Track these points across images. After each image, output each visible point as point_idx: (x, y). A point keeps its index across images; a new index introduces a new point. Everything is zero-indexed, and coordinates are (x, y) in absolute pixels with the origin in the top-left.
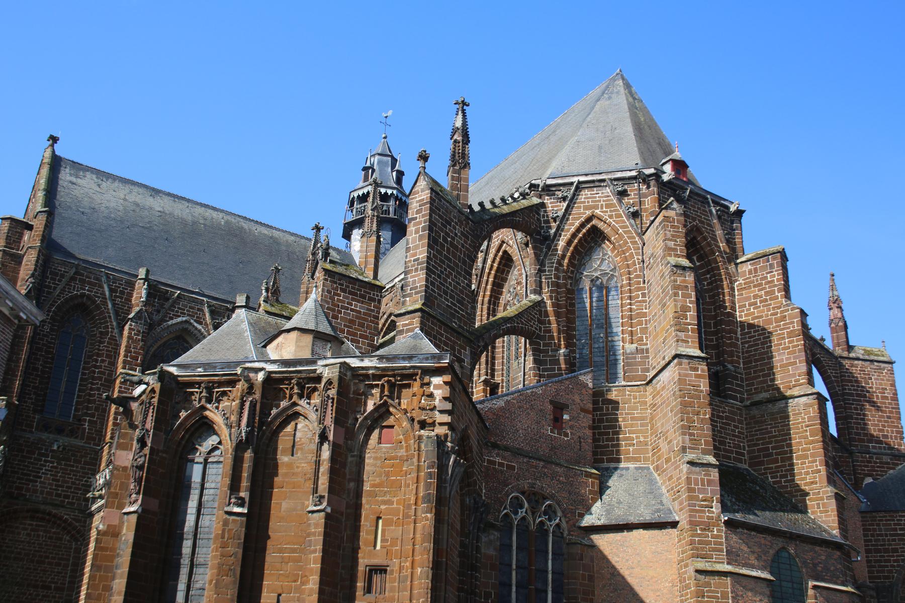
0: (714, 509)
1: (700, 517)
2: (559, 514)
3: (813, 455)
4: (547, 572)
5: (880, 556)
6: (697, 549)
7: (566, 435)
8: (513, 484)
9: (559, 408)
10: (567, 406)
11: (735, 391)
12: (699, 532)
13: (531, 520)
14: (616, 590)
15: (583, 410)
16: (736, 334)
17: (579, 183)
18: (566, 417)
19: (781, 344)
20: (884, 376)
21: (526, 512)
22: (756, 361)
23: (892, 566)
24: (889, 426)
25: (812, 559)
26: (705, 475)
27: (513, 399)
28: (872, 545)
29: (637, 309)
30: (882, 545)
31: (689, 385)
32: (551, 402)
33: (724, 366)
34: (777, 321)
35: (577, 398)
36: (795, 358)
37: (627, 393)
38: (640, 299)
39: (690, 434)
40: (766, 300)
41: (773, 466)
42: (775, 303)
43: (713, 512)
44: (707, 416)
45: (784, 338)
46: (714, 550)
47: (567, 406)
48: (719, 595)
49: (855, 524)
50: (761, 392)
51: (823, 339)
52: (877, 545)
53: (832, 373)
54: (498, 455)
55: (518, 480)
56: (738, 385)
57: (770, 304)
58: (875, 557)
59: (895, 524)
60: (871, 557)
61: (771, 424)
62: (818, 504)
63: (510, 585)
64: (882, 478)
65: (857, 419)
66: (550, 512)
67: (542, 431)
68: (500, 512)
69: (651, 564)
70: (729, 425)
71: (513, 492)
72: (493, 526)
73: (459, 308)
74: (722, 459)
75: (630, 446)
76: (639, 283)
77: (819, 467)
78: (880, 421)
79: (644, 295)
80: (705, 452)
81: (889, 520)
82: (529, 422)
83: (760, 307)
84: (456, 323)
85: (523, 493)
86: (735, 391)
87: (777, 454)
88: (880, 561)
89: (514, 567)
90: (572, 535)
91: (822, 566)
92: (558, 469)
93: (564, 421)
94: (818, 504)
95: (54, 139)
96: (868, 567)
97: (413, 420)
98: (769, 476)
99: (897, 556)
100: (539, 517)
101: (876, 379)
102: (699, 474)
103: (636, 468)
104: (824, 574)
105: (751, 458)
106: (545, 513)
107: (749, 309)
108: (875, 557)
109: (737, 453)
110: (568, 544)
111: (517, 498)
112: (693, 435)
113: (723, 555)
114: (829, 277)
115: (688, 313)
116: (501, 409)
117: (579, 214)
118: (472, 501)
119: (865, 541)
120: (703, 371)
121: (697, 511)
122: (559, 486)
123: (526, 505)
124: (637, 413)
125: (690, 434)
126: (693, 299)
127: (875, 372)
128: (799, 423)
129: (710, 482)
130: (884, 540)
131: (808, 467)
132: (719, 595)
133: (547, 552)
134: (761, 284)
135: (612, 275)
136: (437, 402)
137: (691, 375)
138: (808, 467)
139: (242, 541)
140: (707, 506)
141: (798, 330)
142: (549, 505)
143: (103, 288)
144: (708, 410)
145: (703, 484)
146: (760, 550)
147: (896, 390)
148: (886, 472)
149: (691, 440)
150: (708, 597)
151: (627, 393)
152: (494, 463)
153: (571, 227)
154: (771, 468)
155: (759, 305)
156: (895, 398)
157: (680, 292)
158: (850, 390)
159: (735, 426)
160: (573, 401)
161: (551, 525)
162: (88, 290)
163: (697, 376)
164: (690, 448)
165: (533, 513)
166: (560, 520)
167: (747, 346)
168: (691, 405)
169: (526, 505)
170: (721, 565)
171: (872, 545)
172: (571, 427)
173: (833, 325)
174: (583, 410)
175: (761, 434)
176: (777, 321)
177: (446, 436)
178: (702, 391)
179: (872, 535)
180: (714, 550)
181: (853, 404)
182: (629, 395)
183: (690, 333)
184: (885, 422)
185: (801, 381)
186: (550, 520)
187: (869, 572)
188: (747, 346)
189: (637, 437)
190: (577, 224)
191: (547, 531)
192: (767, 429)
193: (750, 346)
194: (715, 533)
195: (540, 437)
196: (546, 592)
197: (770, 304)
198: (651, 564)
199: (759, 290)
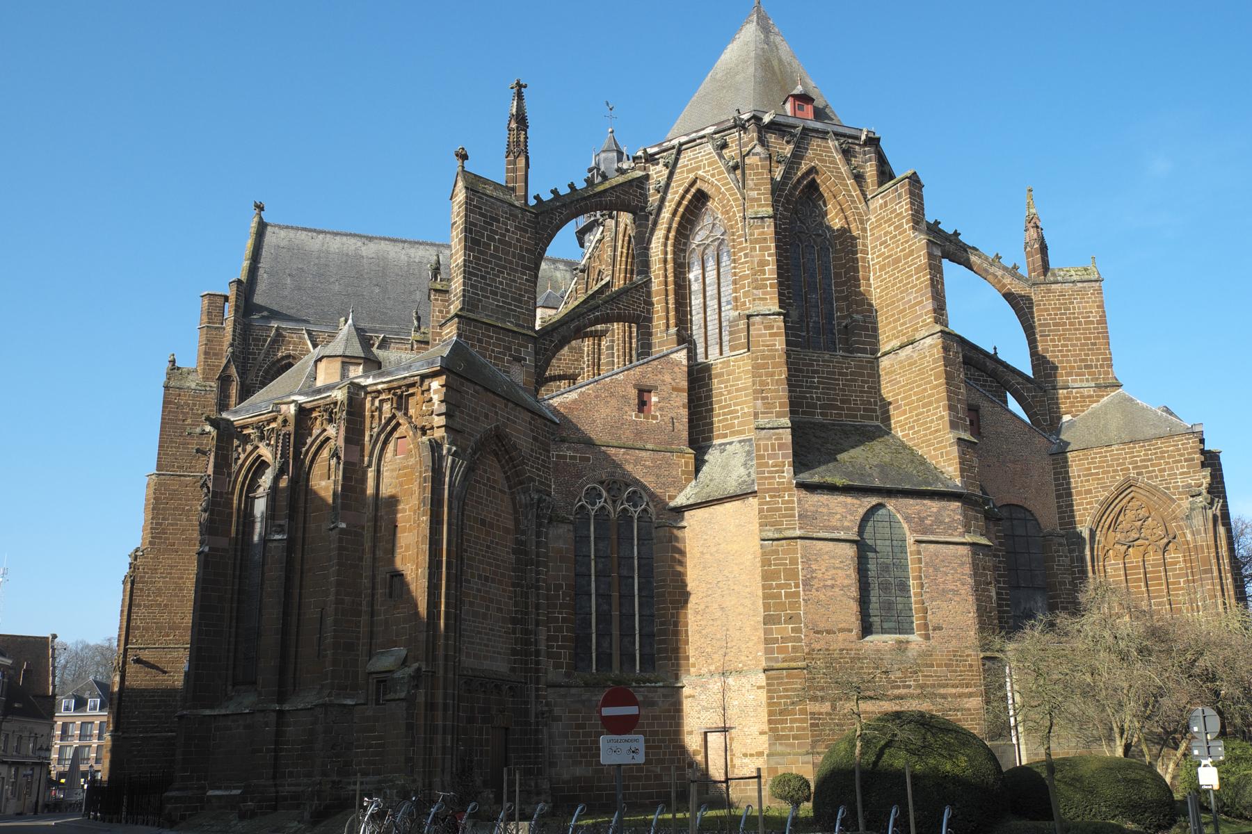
0: (785, 474)
1: (769, 484)
2: (646, 498)
3: (937, 401)
4: (633, 558)
6: (766, 517)
7: (655, 417)
9: (643, 393)
11: (864, 343)
13: (610, 507)
14: (705, 568)
15: (674, 389)
16: (869, 280)
17: (681, 145)
18: (654, 399)
19: (909, 283)
20: (1089, 298)
22: (887, 306)
24: (1092, 355)
25: (918, 514)
26: (775, 439)
27: (588, 389)
29: (739, 273)
31: (763, 346)
32: (635, 386)
33: (852, 318)
34: (906, 257)
35: (668, 378)
36: (921, 296)
37: (732, 363)
38: (743, 260)
39: (763, 398)
41: (902, 418)
42: (903, 238)
43: (784, 477)
44: (783, 376)
45: (912, 276)
46: (785, 516)
47: (656, 388)
48: (788, 562)
49: (1043, 468)
50: (892, 340)
54: (568, 449)
55: (594, 470)
56: (866, 336)
57: (899, 240)
59: (1088, 464)
61: (900, 373)
62: (942, 453)
63: (590, 575)
64: (1082, 414)
65: (1054, 351)
66: (636, 498)
67: (625, 417)
68: (573, 505)
69: (735, 538)
70: (855, 381)
71: (588, 484)
72: (563, 520)
73: (515, 306)
74: (844, 419)
75: (735, 419)
76: (741, 243)
78: (1084, 350)
79: (746, 255)
80: (779, 415)
82: (608, 410)
83: (889, 245)
84: (512, 322)
85: (602, 483)
86: (864, 343)
89: (593, 557)
90: (662, 519)
91: (933, 518)
92: (643, 454)
93: (652, 404)
94: (942, 453)
95: (260, 208)
97: (416, 428)
100: (622, 504)
101: (1077, 303)
102: (765, 438)
103: (740, 442)
104: (935, 527)
106: (629, 499)
107: (880, 250)
109: (865, 410)
110: (656, 528)
111: (594, 488)
112: (767, 398)
115: (766, 268)
116: (575, 401)
118: (528, 498)
120: (779, 328)
121: (766, 478)
122: (644, 471)
123: (604, 494)
124: (742, 384)
125: (763, 398)
126: (773, 251)
127: (1078, 295)
128: (924, 368)
129: (781, 447)
131: (933, 415)
132: (788, 562)
133: (633, 539)
134: (890, 219)
136: (436, 407)
137: (765, 335)
138: (933, 415)
140: (777, 472)
141: (925, 263)
142: (635, 492)
143: (307, 345)
144: (785, 369)
145: (773, 449)
147: (1104, 312)
148: (1089, 405)
149: (764, 404)
150: (775, 565)
151: (732, 363)
152: (565, 457)
153: (673, 197)
156: (1103, 321)
157: (757, 246)
158: (1046, 319)
159: (862, 381)
160: (663, 381)
161: (635, 512)
162: (293, 350)
163: (772, 335)
165: (614, 502)
166: (647, 504)
167: (878, 291)
168: (765, 366)
169: (604, 494)
170: (791, 531)
172: (661, 409)
173: (1028, 249)
174: (674, 389)
175: (892, 386)
176: (906, 257)
177: (443, 437)
178: (776, 350)
180: (785, 516)
181: (1049, 335)
182: (733, 366)
183: (769, 289)
184: (1089, 350)
185: (928, 321)
186: (635, 506)
188: (878, 291)
189: (742, 409)
190: (681, 191)
191: (632, 517)
192: (896, 379)
193: (882, 291)
194: (786, 498)
196: (633, 578)
197: (899, 240)
198: (735, 538)
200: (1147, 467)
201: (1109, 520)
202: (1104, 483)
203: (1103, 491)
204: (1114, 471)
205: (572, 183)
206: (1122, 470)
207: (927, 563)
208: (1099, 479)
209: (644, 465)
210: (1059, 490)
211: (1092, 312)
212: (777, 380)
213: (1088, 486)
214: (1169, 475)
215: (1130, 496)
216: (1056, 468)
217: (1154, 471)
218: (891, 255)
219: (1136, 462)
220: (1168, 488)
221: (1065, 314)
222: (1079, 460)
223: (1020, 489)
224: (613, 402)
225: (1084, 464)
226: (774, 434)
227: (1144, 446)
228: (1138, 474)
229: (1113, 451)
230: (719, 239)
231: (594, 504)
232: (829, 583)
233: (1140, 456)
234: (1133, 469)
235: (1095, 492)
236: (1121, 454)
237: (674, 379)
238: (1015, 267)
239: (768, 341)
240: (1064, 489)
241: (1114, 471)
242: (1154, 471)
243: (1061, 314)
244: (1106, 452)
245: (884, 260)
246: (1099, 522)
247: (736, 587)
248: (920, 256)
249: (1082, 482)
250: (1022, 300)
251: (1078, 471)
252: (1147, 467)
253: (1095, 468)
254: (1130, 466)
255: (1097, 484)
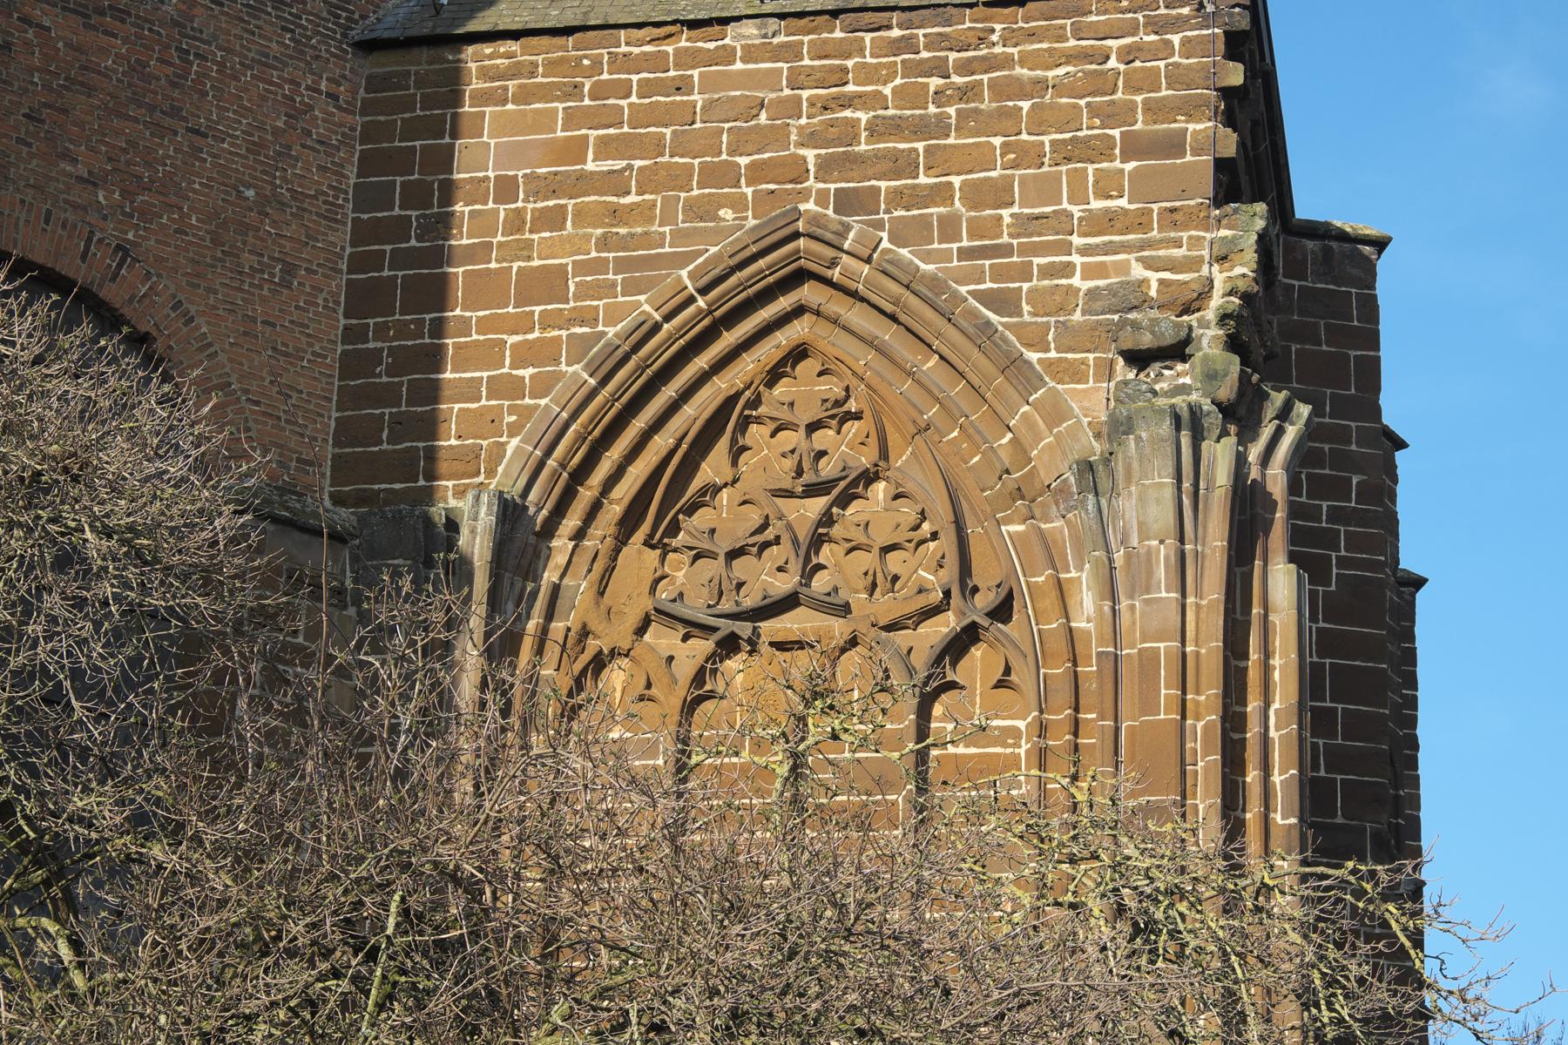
23: (511, 388)
58: (403, 331)
59: (571, 120)
60: (381, 331)
81: (545, 93)
96: (349, 398)
99: (547, 322)
108: (403, 331)
119: (361, 233)
171: (400, 260)
187: (346, 432)
200: (903, 165)
201: (638, 472)
202: (647, 240)
203: (631, 288)
204: (712, 175)
206: (757, 173)
208: (616, 214)
213: (549, 250)
214: (1025, 224)
215: (784, 339)
216: (387, 131)
217: (941, 194)
219: (849, 132)
220: (1004, 302)
222: (524, 96)
223: (91, 182)
225: (548, 118)
227: (908, 45)
228: (847, 203)
229: (727, 56)
233: (878, 100)
234: (826, 168)
235: (584, 292)
236: (770, 81)
240: (402, 259)
241: (712, 175)
242: (941, 194)
244: (688, 59)
246: (580, 475)
249: (516, 223)
251: (509, 155)
252: (903, 165)
253: (606, 148)
254: (810, 154)
255: (604, 243)
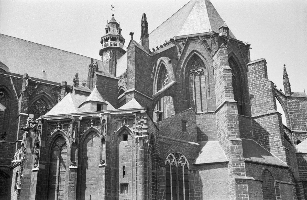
0: (241, 157)
3: (277, 135)
5: (304, 170)
6: (235, 171)
8: (170, 151)
10: (187, 121)
12: (236, 165)
21: (174, 160)
28: (301, 166)
30: (304, 166)
40: (259, 79)
46: (241, 171)
48: (244, 187)
51: (281, 90)
52: (302, 166)
53: (284, 103)
77: (279, 140)
78: (303, 120)
80: (237, 137)
83: (256, 81)
87: (263, 135)
88: (304, 172)
94: (279, 153)
98: (261, 143)
101: (301, 104)
104: (281, 178)
105: (254, 136)
111: (171, 156)
113: (245, 173)
114: (283, 66)
117: (190, 49)
123: (174, 158)
125: (232, 130)
127: (301, 102)
128: (271, 124)
130: (305, 164)
132: (244, 187)
135: (202, 72)
139: (76, 178)
141: (271, 89)
144: (238, 121)
145: (237, 148)
146: (258, 170)
148: (306, 139)
150: (240, 188)
154: (262, 140)
155: (256, 80)
160: (190, 119)
163: (233, 109)
164: (232, 135)
165: (177, 161)
168: (231, 120)
171: (301, 166)
178: (235, 115)
179: (301, 162)
180: (241, 171)
181: (292, 114)
184: (305, 120)
187: (300, 176)
191: (182, 166)
195: (178, 133)
199: (256, 75)
205: (157, 46)
207: (281, 190)
209: (185, 148)
210: (299, 166)
211: (305, 108)
212: (236, 125)
216: (298, 158)
218: (257, 85)
221: (297, 107)
224: (175, 125)
226: (236, 143)
230: (200, 71)
231: (171, 161)
232: (256, 195)
237: (192, 119)
238: (281, 90)
239: (233, 111)
243: (296, 107)
245: (254, 86)
247: (220, 194)
248: (269, 87)
250: (284, 101)
